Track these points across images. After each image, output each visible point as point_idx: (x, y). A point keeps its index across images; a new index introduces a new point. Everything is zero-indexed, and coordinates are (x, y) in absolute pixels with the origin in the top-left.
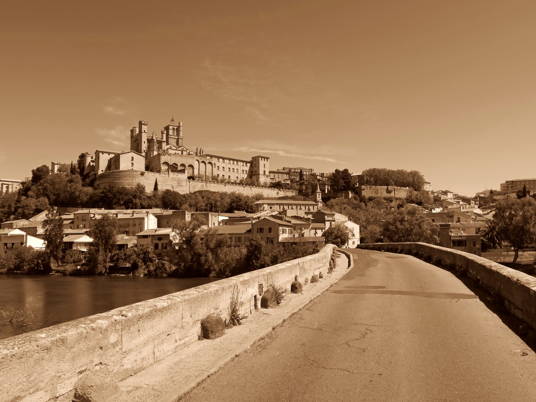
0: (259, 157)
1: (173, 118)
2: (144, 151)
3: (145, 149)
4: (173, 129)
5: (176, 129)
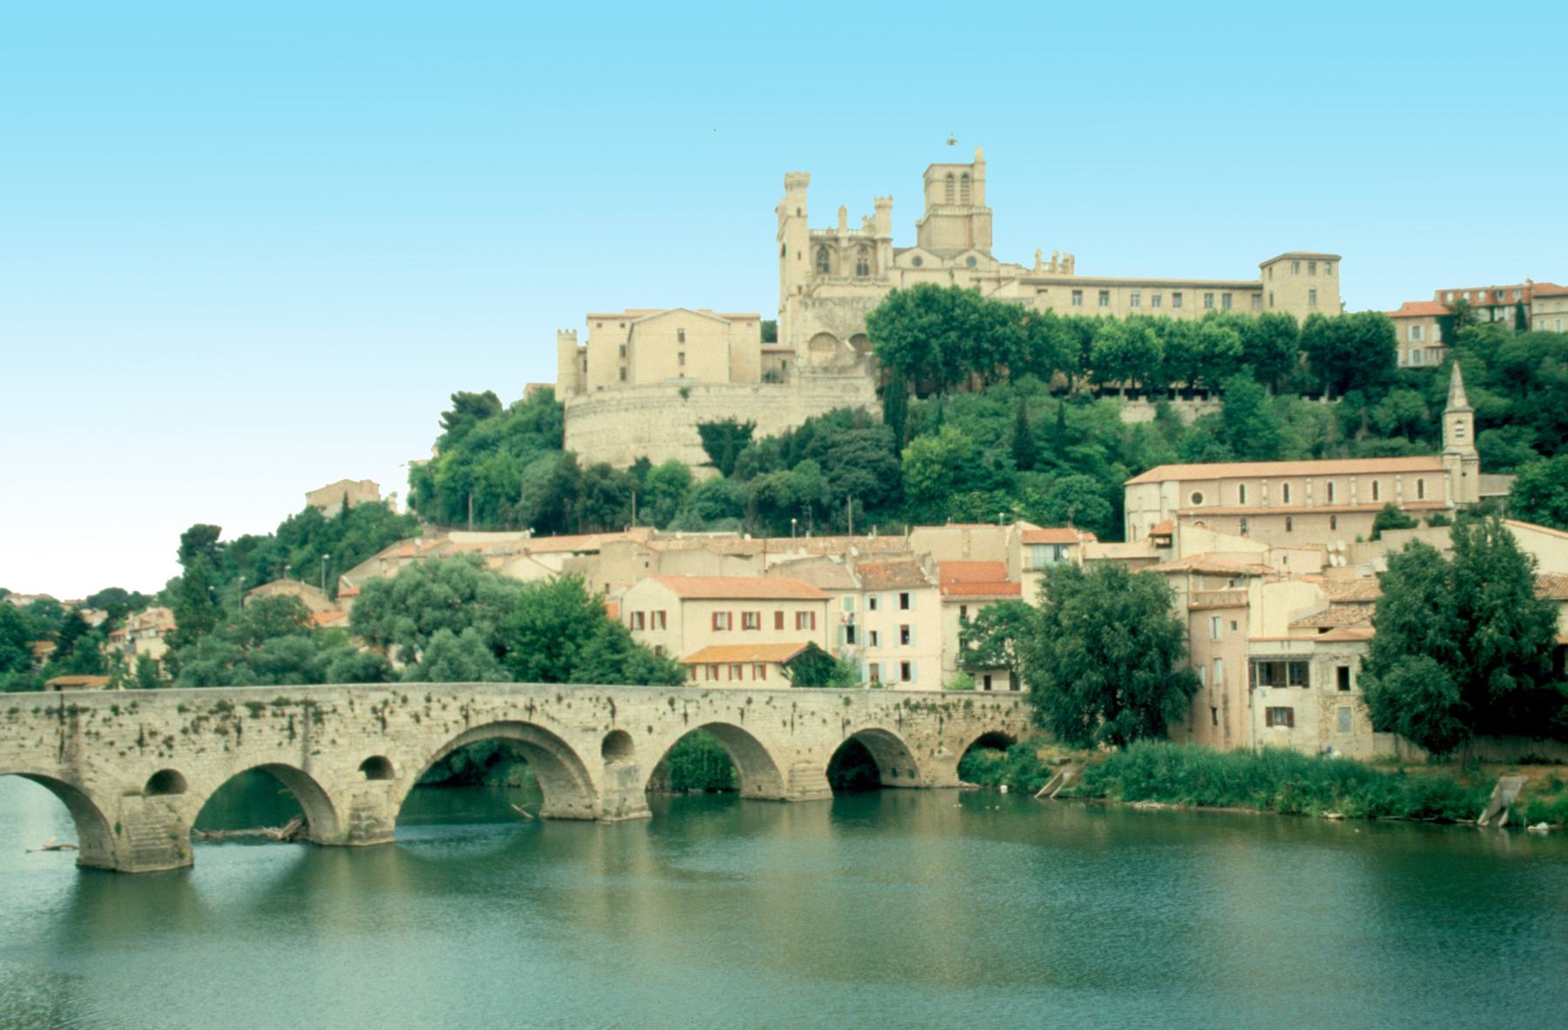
2: (800, 288)
3: (803, 283)
4: (950, 176)
5: (965, 176)
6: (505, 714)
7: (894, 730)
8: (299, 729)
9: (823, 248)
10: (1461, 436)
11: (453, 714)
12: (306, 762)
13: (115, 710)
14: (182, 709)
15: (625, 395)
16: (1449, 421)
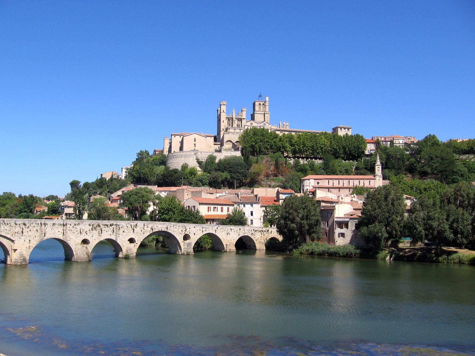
0: (337, 128)
1: (260, 94)
2: (223, 129)
3: (224, 128)
6: (161, 229)
7: (250, 236)
8: (115, 231)
9: (229, 120)
10: (379, 171)
11: (149, 229)
12: (116, 238)
13: (75, 225)
14: (89, 225)
15: (181, 154)
16: (376, 167)
